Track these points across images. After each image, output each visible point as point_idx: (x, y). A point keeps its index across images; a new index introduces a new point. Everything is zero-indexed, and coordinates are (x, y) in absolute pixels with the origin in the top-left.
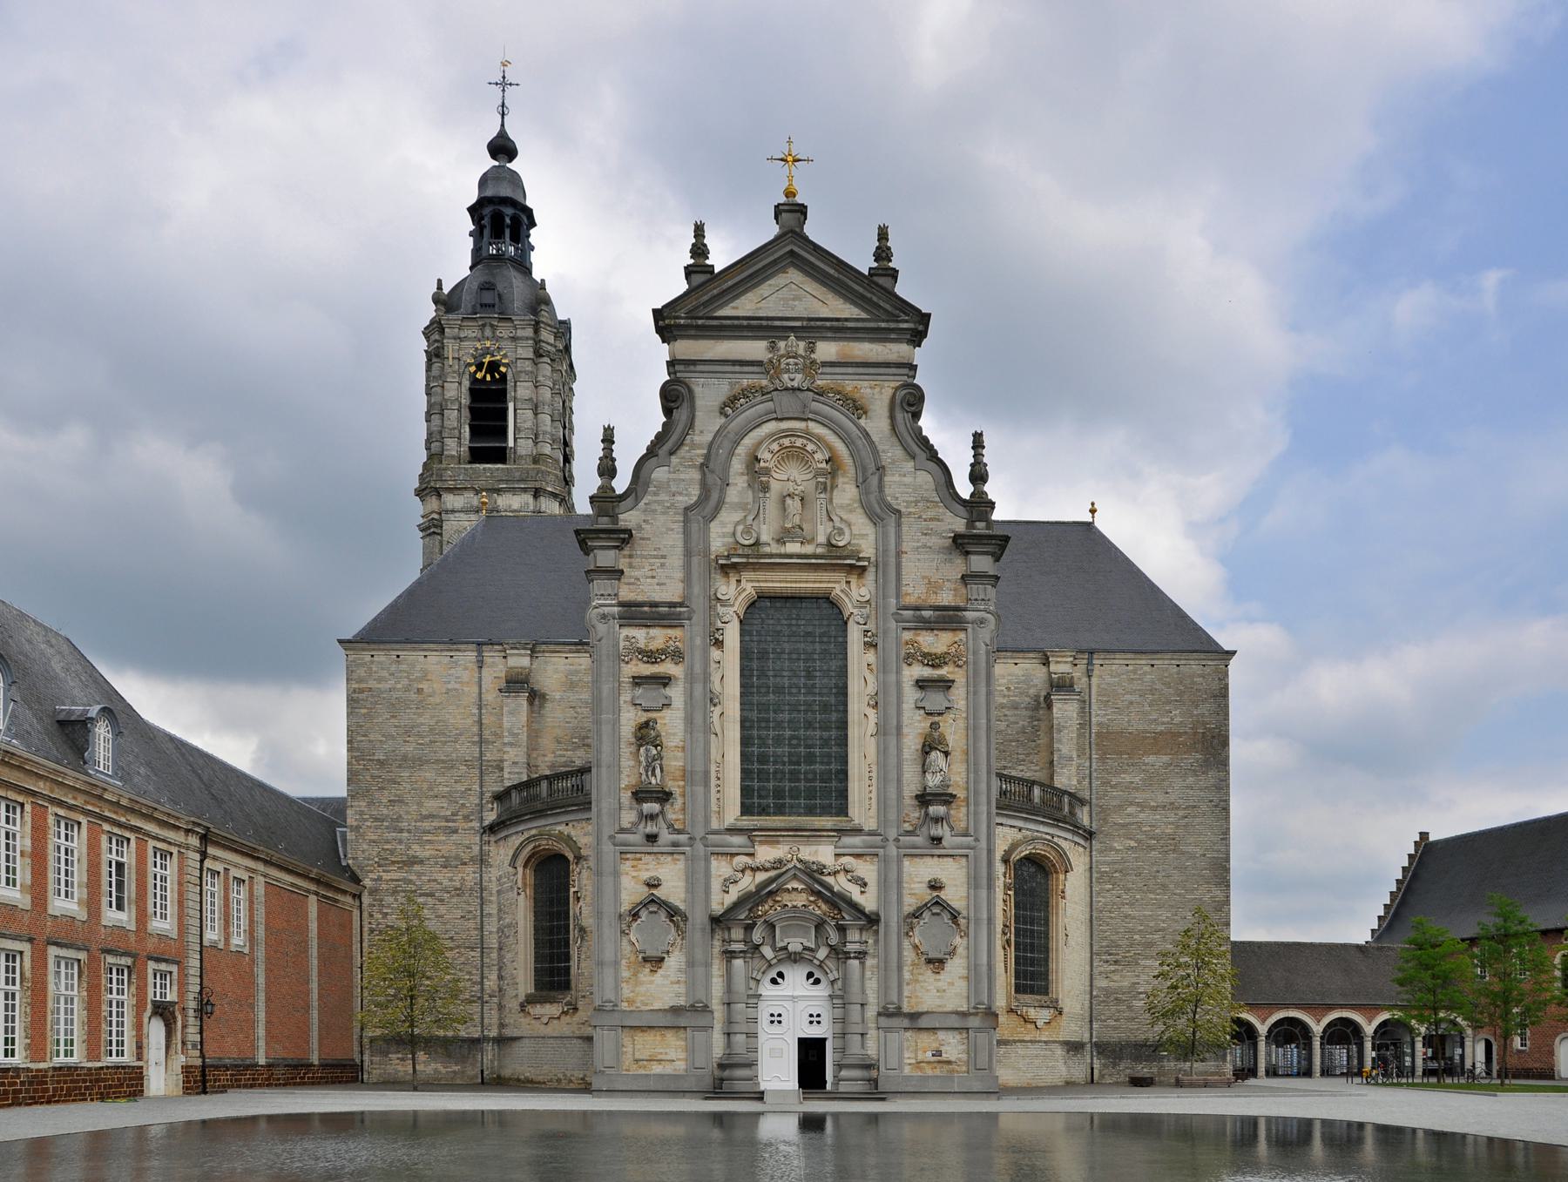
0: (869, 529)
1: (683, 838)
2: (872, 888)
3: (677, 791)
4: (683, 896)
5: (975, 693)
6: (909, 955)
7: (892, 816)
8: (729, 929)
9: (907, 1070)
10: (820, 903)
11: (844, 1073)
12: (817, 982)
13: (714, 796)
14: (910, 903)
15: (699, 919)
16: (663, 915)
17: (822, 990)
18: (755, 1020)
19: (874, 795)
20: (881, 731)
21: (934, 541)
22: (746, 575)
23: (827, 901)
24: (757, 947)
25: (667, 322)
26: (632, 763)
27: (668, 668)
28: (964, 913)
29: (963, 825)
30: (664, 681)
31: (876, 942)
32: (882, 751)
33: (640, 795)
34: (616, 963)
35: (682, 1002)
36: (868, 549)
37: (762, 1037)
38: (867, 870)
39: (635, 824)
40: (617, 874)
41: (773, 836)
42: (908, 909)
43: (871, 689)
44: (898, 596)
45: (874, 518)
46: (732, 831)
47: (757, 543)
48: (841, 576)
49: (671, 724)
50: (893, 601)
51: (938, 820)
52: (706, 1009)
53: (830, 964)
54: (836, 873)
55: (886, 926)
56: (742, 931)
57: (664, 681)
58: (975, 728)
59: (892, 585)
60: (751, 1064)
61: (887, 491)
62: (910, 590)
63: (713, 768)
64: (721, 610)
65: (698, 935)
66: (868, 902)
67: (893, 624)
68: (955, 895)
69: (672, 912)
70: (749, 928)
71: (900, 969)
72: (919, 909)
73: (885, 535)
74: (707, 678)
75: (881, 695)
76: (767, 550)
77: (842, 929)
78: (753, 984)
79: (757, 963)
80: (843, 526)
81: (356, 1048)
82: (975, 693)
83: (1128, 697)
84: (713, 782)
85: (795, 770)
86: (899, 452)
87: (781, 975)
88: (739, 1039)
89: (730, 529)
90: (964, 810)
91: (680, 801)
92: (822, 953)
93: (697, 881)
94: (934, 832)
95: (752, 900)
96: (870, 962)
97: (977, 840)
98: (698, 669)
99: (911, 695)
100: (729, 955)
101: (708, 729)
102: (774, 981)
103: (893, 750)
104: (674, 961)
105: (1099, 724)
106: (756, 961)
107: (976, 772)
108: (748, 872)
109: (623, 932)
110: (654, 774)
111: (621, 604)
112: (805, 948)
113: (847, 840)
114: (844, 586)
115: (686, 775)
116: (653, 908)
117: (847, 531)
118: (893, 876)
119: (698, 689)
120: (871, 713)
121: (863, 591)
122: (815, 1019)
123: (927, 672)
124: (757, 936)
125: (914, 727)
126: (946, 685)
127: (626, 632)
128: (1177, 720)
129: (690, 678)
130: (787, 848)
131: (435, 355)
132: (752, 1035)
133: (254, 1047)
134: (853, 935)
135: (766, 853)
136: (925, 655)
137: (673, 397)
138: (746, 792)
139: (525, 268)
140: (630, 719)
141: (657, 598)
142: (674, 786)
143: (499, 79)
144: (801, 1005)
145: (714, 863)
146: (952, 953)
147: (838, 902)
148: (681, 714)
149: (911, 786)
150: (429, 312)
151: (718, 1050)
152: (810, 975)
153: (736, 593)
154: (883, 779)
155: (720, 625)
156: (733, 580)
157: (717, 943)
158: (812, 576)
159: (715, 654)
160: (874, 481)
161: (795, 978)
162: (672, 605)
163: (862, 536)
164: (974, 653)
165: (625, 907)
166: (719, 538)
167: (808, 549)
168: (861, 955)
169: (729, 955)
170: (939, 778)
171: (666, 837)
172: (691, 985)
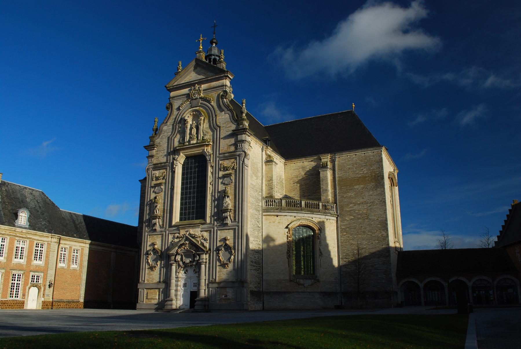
9: (218, 302)
50: (218, 152)
83: (348, 167)
111: (154, 165)
128: (365, 172)
133: (79, 297)
138: (181, 214)
162: (165, 163)
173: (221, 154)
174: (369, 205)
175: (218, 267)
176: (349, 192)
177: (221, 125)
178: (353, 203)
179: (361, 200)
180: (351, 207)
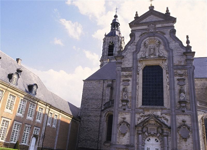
1: (131, 109)
2: (169, 121)
3: (130, 100)
4: (130, 121)
5: (190, 81)
6: (178, 137)
12: (157, 141)
13: (137, 101)
14: (178, 125)
15: (133, 126)
16: (126, 124)
20: (170, 89)
21: (180, 54)
22: (143, 62)
24: (144, 133)
25: (131, 25)
26: (122, 95)
27: (130, 79)
28: (191, 128)
29: (189, 108)
30: (129, 80)
31: (170, 133)
32: (171, 93)
33: (123, 101)
34: (116, 134)
35: (128, 143)
36: (166, 56)
38: (168, 117)
39: (122, 107)
40: (117, 116)
41: (148, 110)
42: (178, 126)
43: (168, 81)
44: (173, 64)
46: (140, 108)
47: (146, 57)
49: (129, 88)
50: (172, 65)
52: (133, 146)
54: (161, 118)
55: (173, 129)
57: (129, 80)
59: (172, 62)
61: (170, 46)
62: (175, 63)
65: (132, 129)
66: (168, 124)
67: (172, 69)
68: (188, 123)
69: (128, 124)
71: (176, 139)
72: (180, 126)
73: (170, 54)
74: (136, 80)
76: (147, 57)
82: (190, 81)
85: (153, 95)
86: (172, 40)
87: (149, 139)
91: (130, 102)
93: (133, 118)
94: (183, 110)
95: (143, 122)
96: (169, 138)
97: (193, 111)
98: (134, 78)
99: (176, 82)
100: (138, 134)
101: (136, 89)
102: (148, 140)
104: (127, 135)
108: (143, 117)
109: (118, 128)
110: (125, 97)
112: (154, 133)
113: (164, 111)
115: (132, 98)
116: (124, 123)
118: (174, 119)
119: (134, 82)
120: (168, 86)
123: (180, 78)
125: (177, 88)
126: (184, 79)
127: (122, 73)
129: (133, 80)
131: (104, 42)
135: (147, 113)
136: (179, 74)
137: (132, 35)
138: (143, 101)
139: (117, 30)
140: (122, 87)
141: (127, 67)
142: (129, 100)
144: (154, 146)
146: (189, 137)
148: (131, 86)
149: (177, 101)
150: (104, 37)
152: (156, 140)
153: (141, 66)
154: (171, 99)
157: (136, 131)
159: (138, 76)
161: (153, 140)
163: (165, 54)
165: (119, 123)
167: (155, 57)
168: (167, 136)
169: (138, 134)
170: (183, 98)
171: (127, 109)
172: (130, 140)
173: (174, 66)
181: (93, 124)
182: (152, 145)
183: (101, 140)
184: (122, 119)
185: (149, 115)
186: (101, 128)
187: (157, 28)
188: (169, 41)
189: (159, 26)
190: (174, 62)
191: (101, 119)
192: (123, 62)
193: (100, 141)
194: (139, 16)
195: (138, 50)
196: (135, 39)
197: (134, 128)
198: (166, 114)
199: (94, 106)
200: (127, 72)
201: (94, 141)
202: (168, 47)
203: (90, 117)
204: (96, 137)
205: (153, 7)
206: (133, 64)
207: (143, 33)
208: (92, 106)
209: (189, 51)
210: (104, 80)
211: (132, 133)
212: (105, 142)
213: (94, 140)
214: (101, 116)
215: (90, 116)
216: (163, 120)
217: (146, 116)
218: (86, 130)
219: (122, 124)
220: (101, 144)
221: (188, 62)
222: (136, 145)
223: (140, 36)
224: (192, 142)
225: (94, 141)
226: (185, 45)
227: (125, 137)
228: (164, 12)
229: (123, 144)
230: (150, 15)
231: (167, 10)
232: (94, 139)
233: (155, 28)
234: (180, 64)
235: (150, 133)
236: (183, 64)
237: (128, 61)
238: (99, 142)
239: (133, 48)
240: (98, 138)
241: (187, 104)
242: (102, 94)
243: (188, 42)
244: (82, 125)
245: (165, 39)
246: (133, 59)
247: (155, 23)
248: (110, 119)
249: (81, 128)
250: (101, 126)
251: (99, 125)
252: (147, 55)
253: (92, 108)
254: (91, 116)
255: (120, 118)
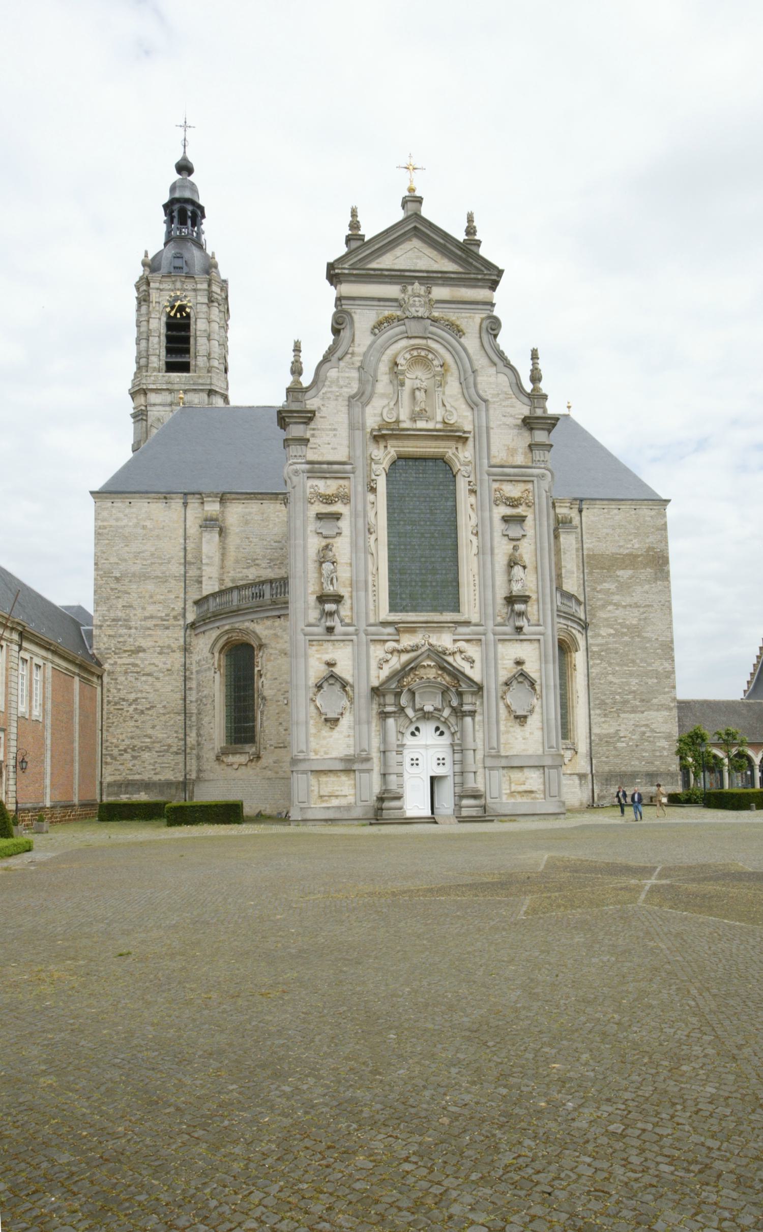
0: (468, 413)
7: (490, 610)
8: (384, 696)
10: (445, 675)
11: (465, 802)
12: (442, 734)
13: (371, 598)
17: (446, 740)
18: (400, 764)
19: (477, 597)
22: (391, 443)
23: (449, 673)
32: (482, 566)
37: (406, 776)
44: (489, 458)
45: (472, 406)
47: (398, 421)
48: (453, 444)
51: (521, 614)
53: (453, 720)
54: (454, 653)
56: (393, 697)
58: (542, 549)
60: (399, 798)
61: (479, 386)
63: (370, 578)
64: (374, 466)
70: (398, 695)
75: (480, 525)
77: (460, 694)
78: (400, 736)
79: (402, 720)
80: (452, 410)
81: (98, 791)
82: (540, 525)
84: (370, 588)
87: (417, 729)
88: (392, 778)
89: (378, 411)
90: (535, 607)
92: (446, 712)
93: (360, 660)
94: (518, 624)
100: (384, 716)
102: (413, 734)
103: (489, 566)
104: (346, 721)
105: (588, 549)
106: (402, 719)
107: (543, 580)
108: (395, 654)
112: (436, 709)
113: (462, 630)
114: (454, 450)
117: (454, 412)
118: (492, 655)
121: (467, 454)
122: (441, 762)
123: (509, 511)
124: (404, 701)
130: (421, 636)
132: (400, 775)
134: (468, 699)
136: (507, 499)
138: (392, 595)
143: (182, 123)
144: (431, 751)
145: (372, 647)
147: (457, 675)
151: (376, 789)
152: (437, 729)
153: (384, 455)
155: (374, 477)
156: (382, 446)
157: (375, 706)
158: (434, 443)
159: (371, 497)
160: (471, 380)
161: (427, 730)
164: (539, 498)
166: (374, 415)
167: (430, 425)
169: (384, 716)
174: (642, 610)
175: (502, 723)
176: (605, 582)
177: (489, 397)
178: (615, 604)
179: (628, 600)
180: (609, 611)
181: (158, 685)
182: (426, 747)
183: (199, 744)
184: (323, 667)
185: (415, 648)
186: (192, 696)
187: (438, 302)
188: (477, 366)
189: (440, 292)
190: (494, 451)
191: (188, 662)
192: (313, 436)
193: (191, 749)
194: (369, 231)
195: (369, 388)
196: (353, 341)
197: (369, 695)
198: (467, 641)
199: (151, 609)
200: (329, 482)
201: (167, 751)
202: (472, 390)
203: (141, 655)
204: (176, 732)
205: (419, 200)
206: (351, 445)
207: (389, 320)
208: (144, 609)
209: (539, 412)
210: (185, 494)
211: (364, 715)
212: (225, 752)
213: (170, 746)
214: (186, 649)
215: (140, 650)
216: (458, 662)
217: (406, 651)
218: (131, 709)
219: (325, 685)
220: (199, 758)
221: (538, 454)
222: (375, 755)
223: (375, 327)
224: (540, 724)
225: (167, 751)
226: (528, 387)
227: (337, 729)
228: (461, 236)
229: (334, 754)
230: (409, 239)
231: (471, 231)
232: (169, 741)
233: (432, 303)
234: (511, 458)
235: (422, 709)
236: (519, 459)
237: (332, 433)
238: (188, 751)
239: (344, 378)
240: (185, 740)
241: (529, 604)
242: (182, 554)
243: (536, 378)
244: (109, 691)
245: (463, 354)
246: (352, 427)
247: (430, 278)
248: (241, 660)
249: (109, 702)
250: (190, 689)
251: (180, 684)
252: (404, 414)
253: (146, 618)
254: (144, 651)
255: (316, 670)
